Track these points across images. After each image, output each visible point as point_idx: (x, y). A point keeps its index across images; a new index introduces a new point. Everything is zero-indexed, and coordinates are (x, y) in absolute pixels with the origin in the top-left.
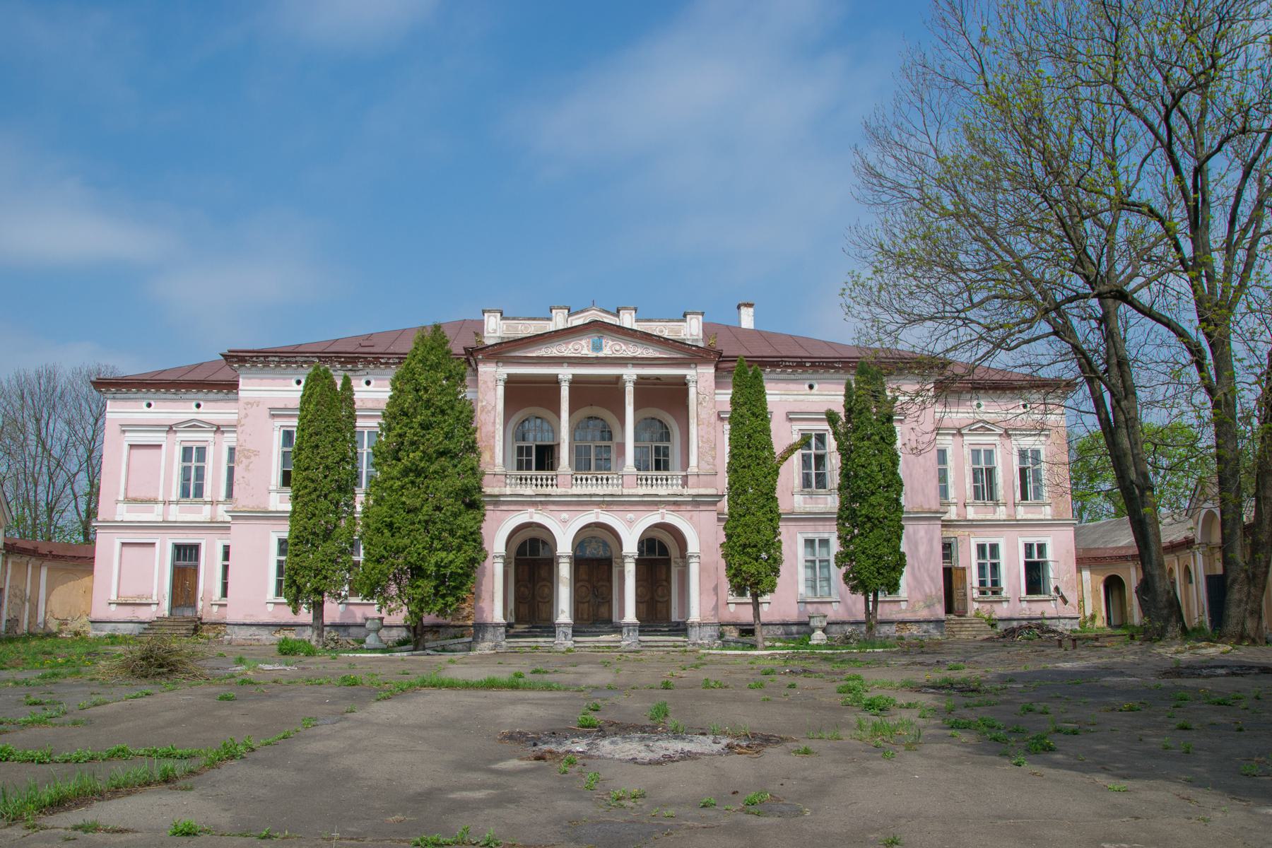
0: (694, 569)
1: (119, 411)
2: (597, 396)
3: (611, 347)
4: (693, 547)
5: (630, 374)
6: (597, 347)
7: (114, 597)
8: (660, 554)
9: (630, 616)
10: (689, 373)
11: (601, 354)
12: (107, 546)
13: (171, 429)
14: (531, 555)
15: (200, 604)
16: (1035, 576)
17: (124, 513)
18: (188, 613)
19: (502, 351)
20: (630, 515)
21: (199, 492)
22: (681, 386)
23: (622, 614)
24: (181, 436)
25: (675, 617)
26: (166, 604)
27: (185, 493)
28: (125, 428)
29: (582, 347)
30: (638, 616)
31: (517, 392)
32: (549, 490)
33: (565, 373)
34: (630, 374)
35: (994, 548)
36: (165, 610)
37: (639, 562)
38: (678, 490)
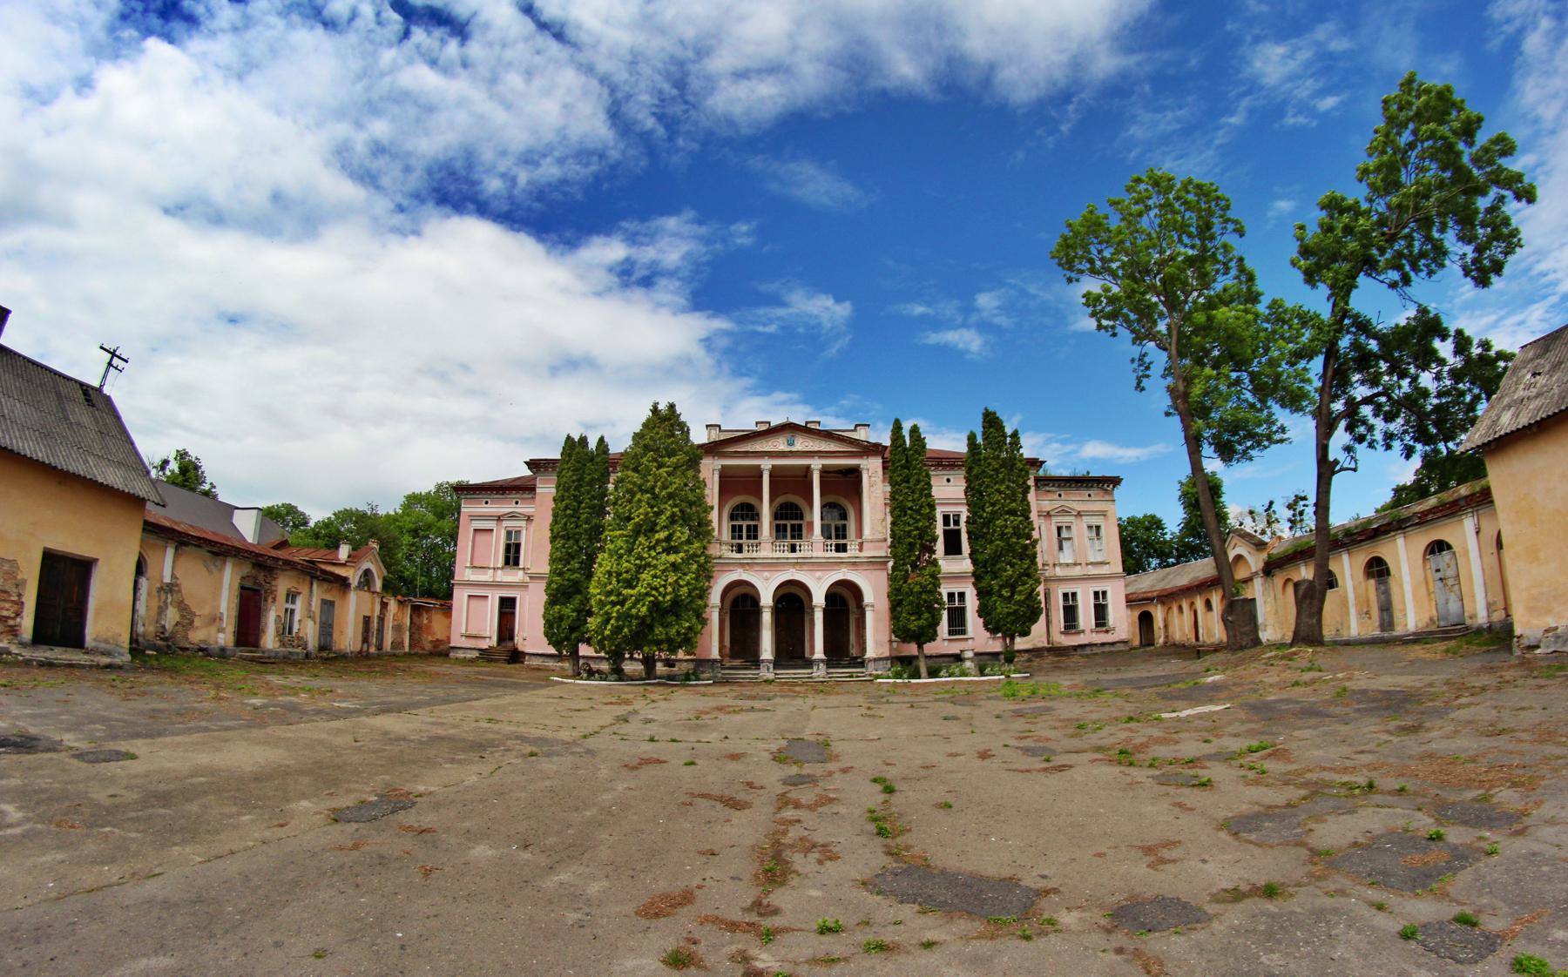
0: (869, 616)
1: (467, 509)
2: (791, 483)
3: (801, 444)
4: (868, 598)
5: (816, 464)
6: (791, 444)
8: (844, 600)
9: (819, 653)
11: (794, 449)
12: (460, 597)
13: (499, 519)
14: (742, 603)
16: (1100, 611)
18: (510, 644)
20: (818, 574)
21: (516, 563)
22: (854, 474)
23: (812, 652)
25: (854, 652)
26: (495, 638)
27: (507, 562)
28: (474, 517)
29: (780, 444)
30: (825, 653)
31: (730, 482)
32: (754, 555)
33: (766, 464)
34: (816, 464)
35: (1074, 595)
36: (494, 642)
37: (825, 611)
38: (857, 553)
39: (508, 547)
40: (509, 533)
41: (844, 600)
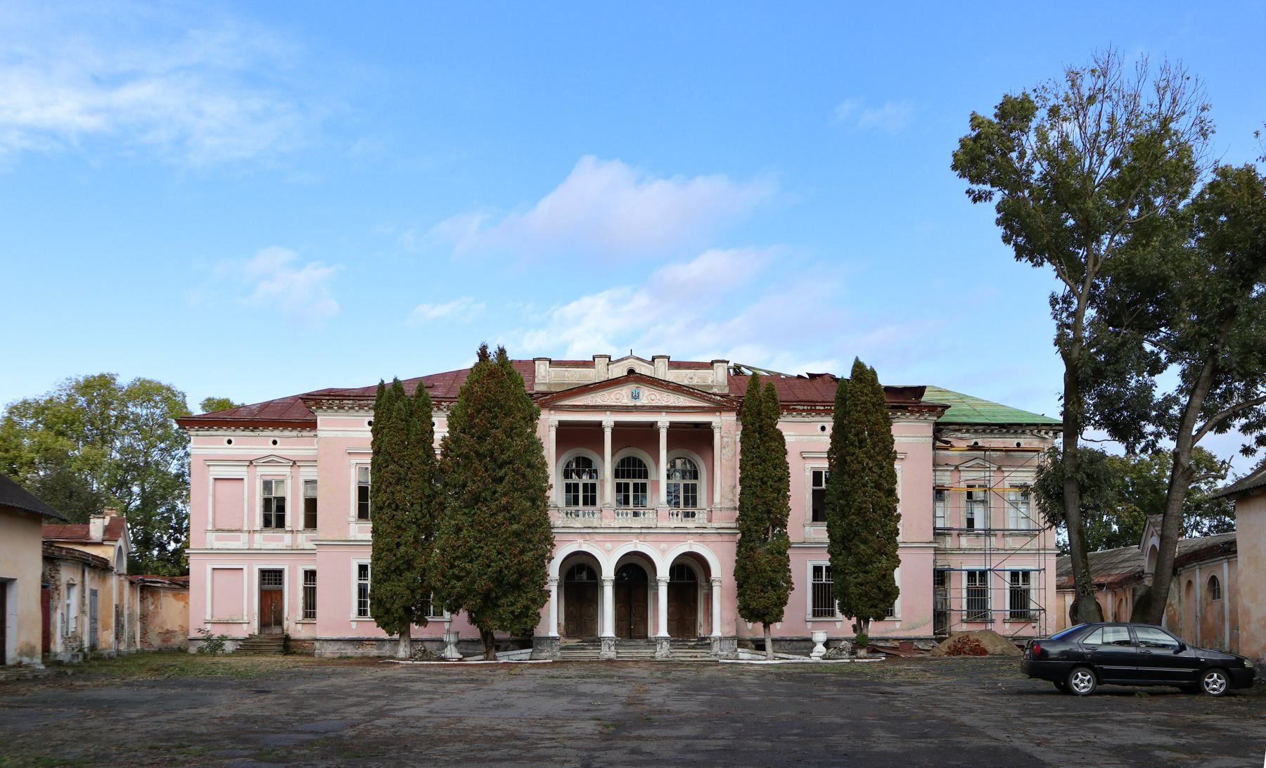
2: (636, 436)
4: (716, 572)
5: (663, 420)
6: (636, 397)
7: (208, 618)
8: (690, 574)
10: (715, 419)
11: (638, 403)
15: (286, 623)
17: (213, 541)
19: (552, 399)
21: (281, 523)
24: (261, 470)
27: (267, 523)
33: (608, 420)
34: (663, 420)
36: (254, 628)
37: (670, 586)
39: (267, 503)
40: (267, 485)
41: (690, 574)
